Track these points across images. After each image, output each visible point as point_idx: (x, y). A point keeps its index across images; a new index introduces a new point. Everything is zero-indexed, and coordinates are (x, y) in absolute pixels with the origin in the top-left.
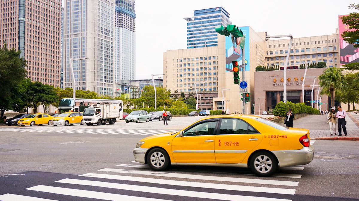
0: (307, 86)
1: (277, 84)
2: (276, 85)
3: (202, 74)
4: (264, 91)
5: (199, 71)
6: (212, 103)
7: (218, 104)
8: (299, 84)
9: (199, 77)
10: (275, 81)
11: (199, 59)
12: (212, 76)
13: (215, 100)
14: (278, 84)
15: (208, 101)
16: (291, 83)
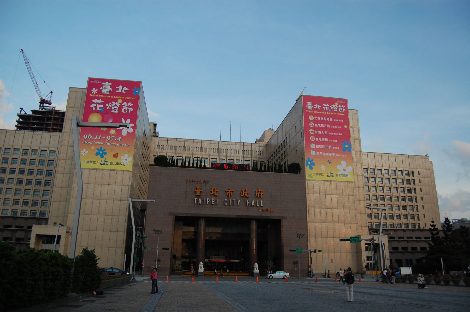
0: (267, 210)
1: (202, 201)
2: (200, 202)
3: (20, 182)
4: (170, 214)
5: (16, 176)
6: (30, 239)
7: (44, 243)
8: (251, 203)
9: (13, 186)
10: (198, 194)
11: (20, 152)
12: (41, 188)
13: (37, 230)
14: (206, 201)
15: (20, 234)
16: (234, 200)
